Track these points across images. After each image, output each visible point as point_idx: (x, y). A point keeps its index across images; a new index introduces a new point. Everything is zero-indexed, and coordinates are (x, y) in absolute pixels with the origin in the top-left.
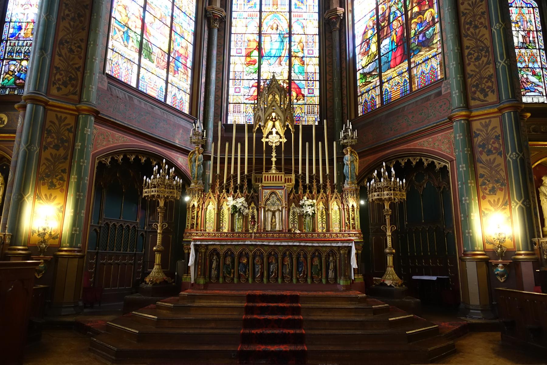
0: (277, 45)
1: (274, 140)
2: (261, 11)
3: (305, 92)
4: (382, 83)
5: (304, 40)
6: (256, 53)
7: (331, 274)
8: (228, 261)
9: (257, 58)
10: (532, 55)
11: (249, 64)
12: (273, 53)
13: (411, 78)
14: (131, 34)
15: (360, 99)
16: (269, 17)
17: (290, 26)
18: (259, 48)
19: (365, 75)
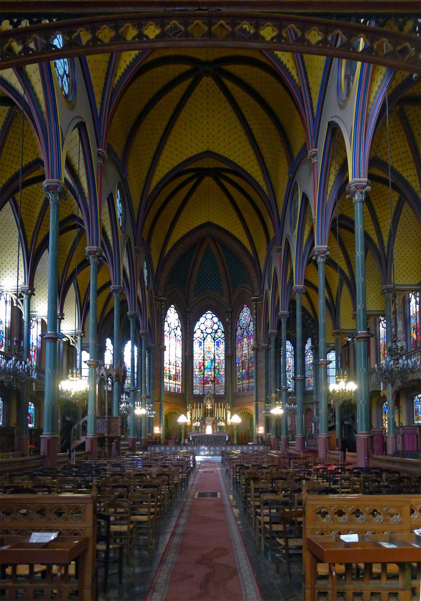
0: (210, 364)
1: (209, 407)
2: (204, 351)
3: (220, 382)
4: (243, 384)
5: (219, 362)
6: (202, 367)
7: (222, 442)
8: (199, 439)
9: (203, 369)
10: (290, 374)
11: (200, 372)
12: (209, 367)
13: (249, 386)
14: (167, 375)
15: (237, 387)
16: (207, 353)
17: (214, 357)
18: (204, 365)
19: (239, 379)
